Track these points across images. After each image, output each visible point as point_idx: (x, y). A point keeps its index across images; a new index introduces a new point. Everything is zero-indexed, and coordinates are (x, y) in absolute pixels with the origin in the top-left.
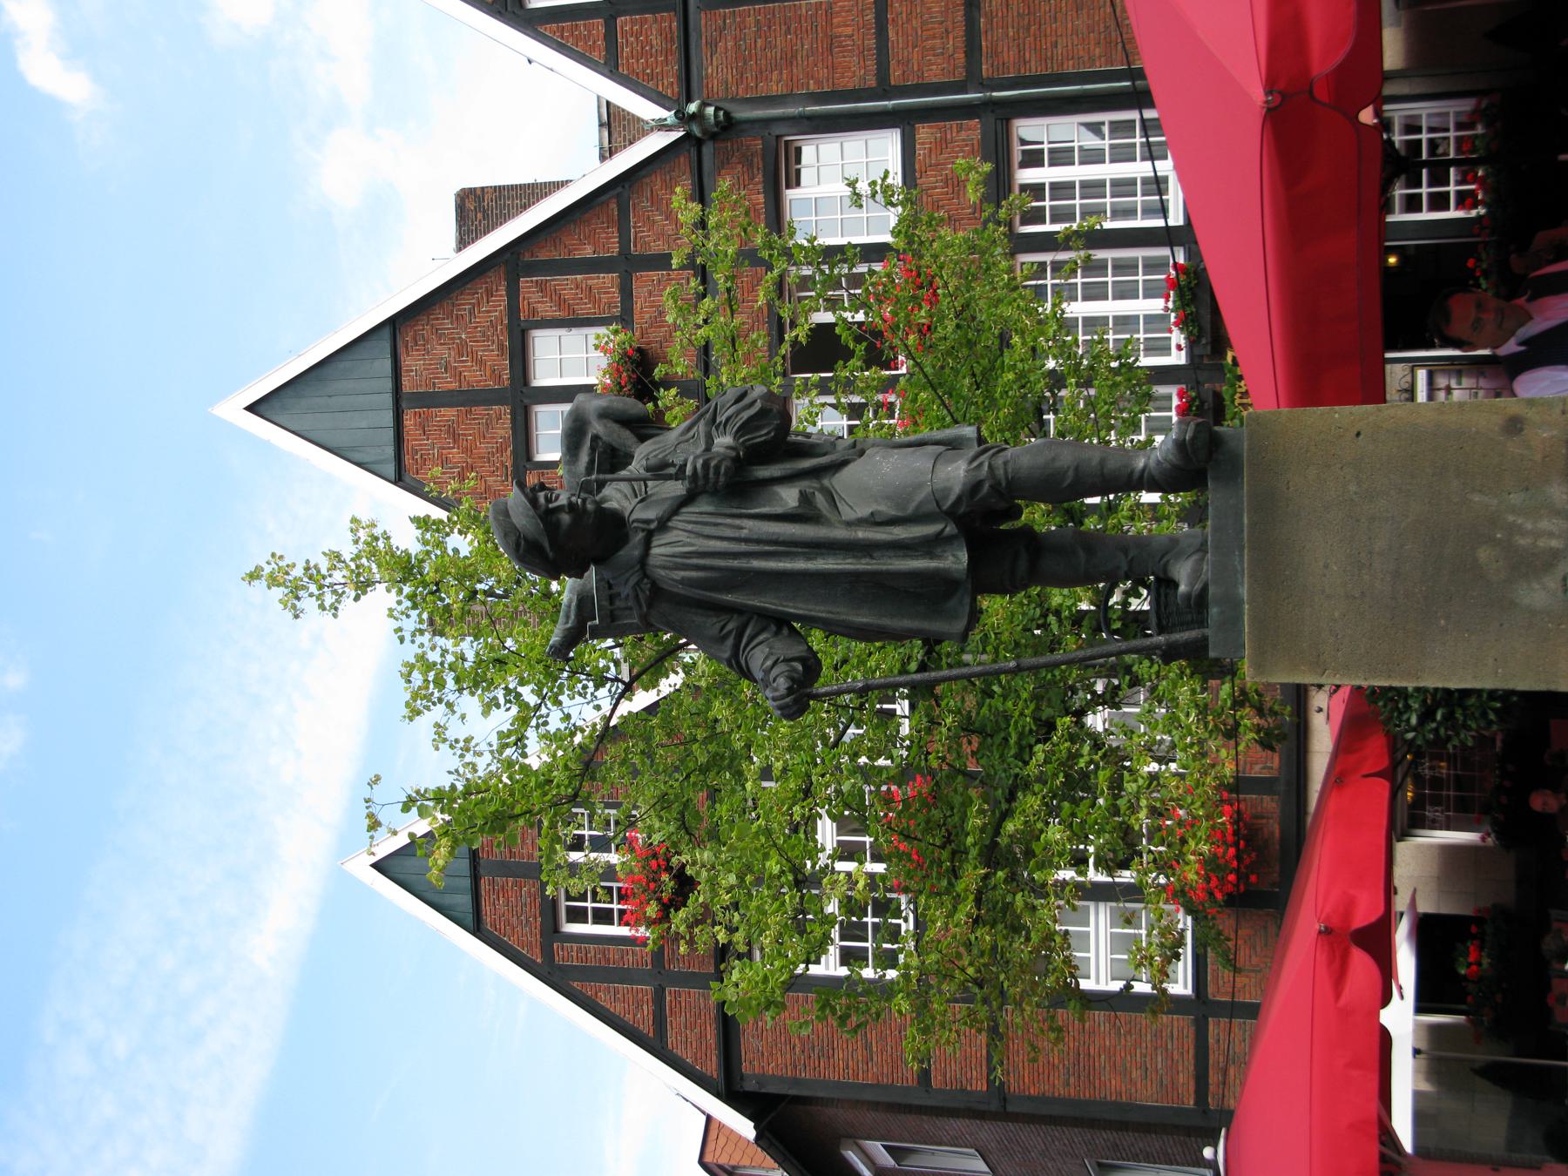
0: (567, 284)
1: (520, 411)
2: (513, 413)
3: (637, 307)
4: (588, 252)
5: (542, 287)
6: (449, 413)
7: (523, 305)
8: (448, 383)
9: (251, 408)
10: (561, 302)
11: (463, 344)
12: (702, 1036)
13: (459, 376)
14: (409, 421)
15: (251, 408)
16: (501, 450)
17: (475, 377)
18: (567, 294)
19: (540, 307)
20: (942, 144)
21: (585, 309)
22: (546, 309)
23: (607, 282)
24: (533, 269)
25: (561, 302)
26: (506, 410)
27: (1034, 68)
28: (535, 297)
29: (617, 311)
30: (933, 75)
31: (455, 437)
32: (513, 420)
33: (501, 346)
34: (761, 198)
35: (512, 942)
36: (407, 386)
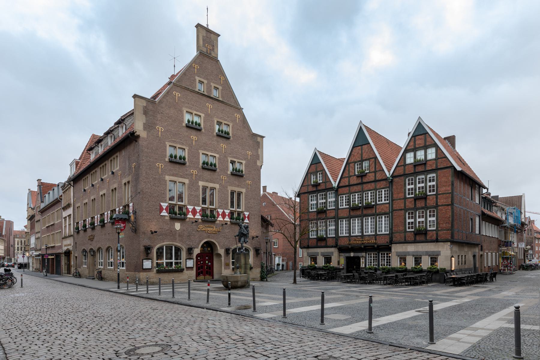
0: (373, 165)
6: (360, 152)
8: (363, 151)
14: (360, 147)
17: (364, 154)
20: (387, 207)
22: (371, 162)
23: (374, 170)
24: (375, 160)
27: (394, 217)
30: (394, 206)
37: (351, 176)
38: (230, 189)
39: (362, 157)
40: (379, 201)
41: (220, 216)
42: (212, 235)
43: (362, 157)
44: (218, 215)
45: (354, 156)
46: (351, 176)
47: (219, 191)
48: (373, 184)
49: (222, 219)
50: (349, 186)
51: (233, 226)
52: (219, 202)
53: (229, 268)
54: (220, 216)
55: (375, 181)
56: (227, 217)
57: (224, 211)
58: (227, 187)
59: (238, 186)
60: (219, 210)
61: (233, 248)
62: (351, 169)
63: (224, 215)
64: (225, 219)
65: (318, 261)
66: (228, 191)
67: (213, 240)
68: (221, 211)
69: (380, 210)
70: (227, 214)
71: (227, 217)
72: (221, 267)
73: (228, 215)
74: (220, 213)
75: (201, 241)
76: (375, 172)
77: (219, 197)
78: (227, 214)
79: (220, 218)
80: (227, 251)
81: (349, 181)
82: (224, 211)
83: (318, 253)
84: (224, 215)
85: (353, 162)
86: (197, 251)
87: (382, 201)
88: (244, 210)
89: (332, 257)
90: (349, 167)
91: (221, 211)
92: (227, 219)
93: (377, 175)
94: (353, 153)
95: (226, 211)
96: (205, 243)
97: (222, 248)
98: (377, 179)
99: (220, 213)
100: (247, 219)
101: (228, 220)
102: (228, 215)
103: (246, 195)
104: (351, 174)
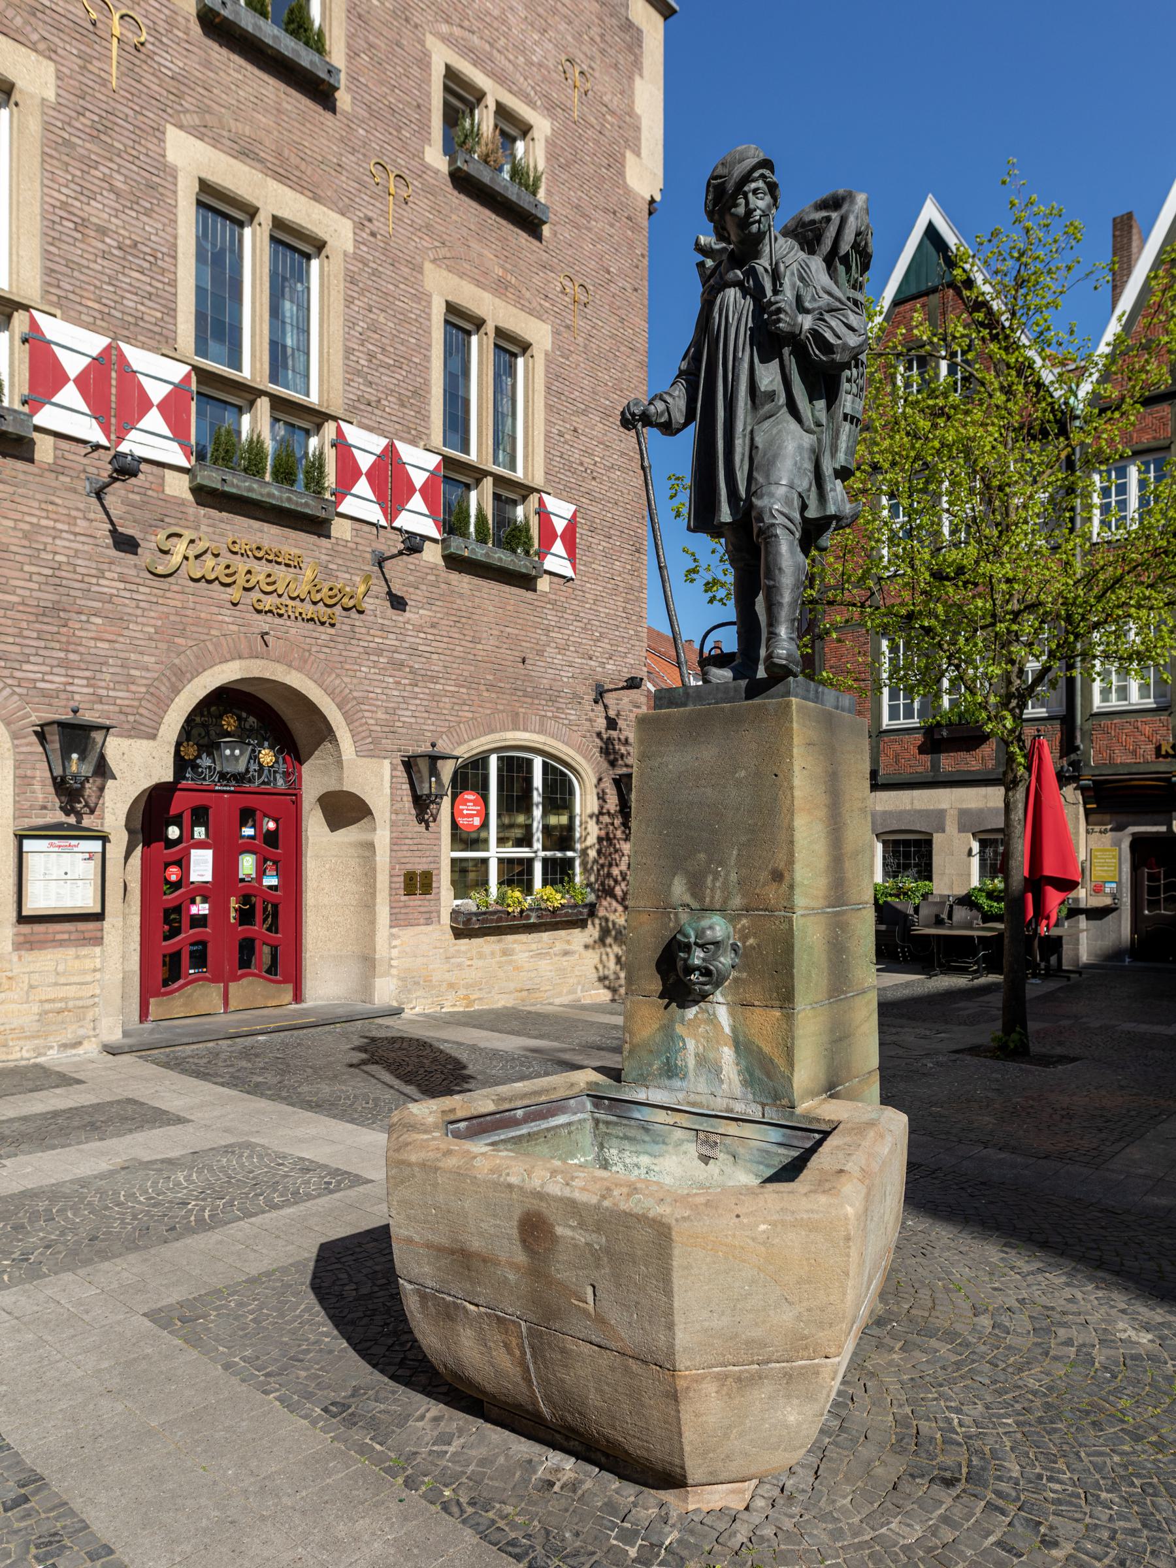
38: (442, 286)
41: (362, 487)
42: (296, 630)
44: (349, 472)
47: (351, 279)
49: (373, 513)
51: (464, 582)
52: (352, 372)
53: (430, 918)
54: (362, 487)
56: (417, 502)
57: (390, 450)
58: (419, 269)
59: (501, 288)
60: (354, 434)
61: (466, 750)
63: (390, 481)
64: (405, 521)
65: (938, 860)
66: (423, 298)
67: (296, 680)
68: (367, 445)
70: (419, 478)
71: (417, 502)
72: (368, 906)
73: (427, 492)
74: (365, 462)
75: (180, 678)
77: (350, 323)
78: (419, 478)
79: (361, 503)
80: (417, 767)
82: (390, 450)
83: (941, 814)
84: (390, 481)
86: (140, 762)
88: (538, 480)
89: (937, 839)
91: (367, 445)
92: (417, 518)
95: (408, 453)
96: (224, 699)
97: (371, 749)
99: (365, 462)
100: (558, 547)
101: (428, 527)
102: (427, 492)
103: (555, 377)
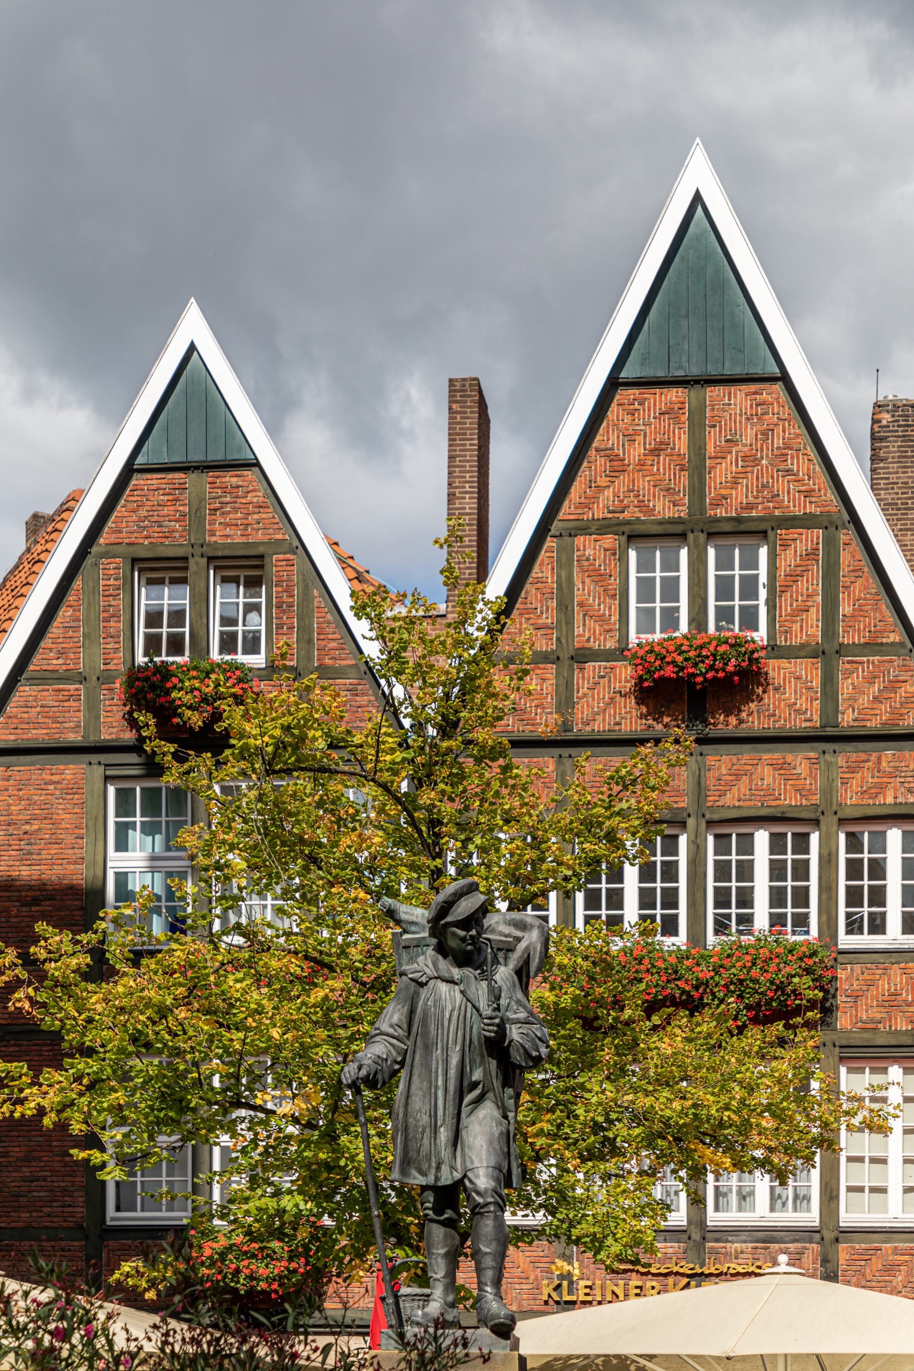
0: (812, 583)
1: (679, 529)
2: (679, 521)
3: (784, 663)
4: (845, 608)
5: (811, 555)
6: (682, 443)
7: (793, 533)
8: (713, 441)
9: (697, 199)
10: (794, 577)
11: (756, 461)
12: (37, 725)
13: (721, 456)
15: (697, 199)
16: (642, 506)
17: (720, 474)
18: (802, 585)
19: (790, 553)
21: (785, 605)
22: (788, 559)
23: (811, 628)
24: (831, 544)
25: (794, 577)
26: (682, 512)
28: (801, 547)
29: (781, 641)
31: (655, 452)
32: (672, 521)
33: (750, 507)
34: (890, 800)
35: (120, 510)
36: (712, 393)
37: (582, 657)
39: (698, 490)
40: (854, 927)
43: (698, 490)
45: (617, 466)
46: (582, 657)
48: (800, 760)
50: (565, 743)
55: (827, 738)
62: (584, 589)
69: (869, 1011)
76: (828, 653)
81: (566, 700)
85: (604, 527)
87: (878, 926)
90: (565, 562)
93: (845, 688)
94: (605, 437)
98: (847, 719)
104: (585, 632)
